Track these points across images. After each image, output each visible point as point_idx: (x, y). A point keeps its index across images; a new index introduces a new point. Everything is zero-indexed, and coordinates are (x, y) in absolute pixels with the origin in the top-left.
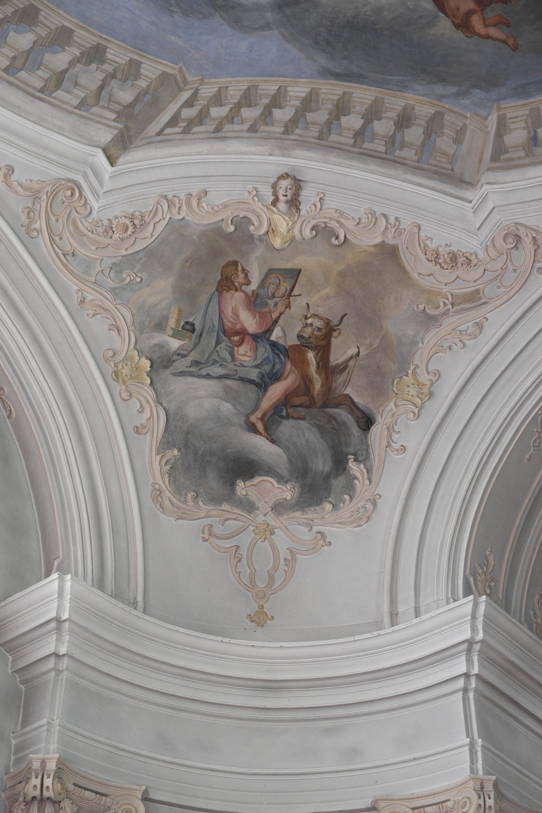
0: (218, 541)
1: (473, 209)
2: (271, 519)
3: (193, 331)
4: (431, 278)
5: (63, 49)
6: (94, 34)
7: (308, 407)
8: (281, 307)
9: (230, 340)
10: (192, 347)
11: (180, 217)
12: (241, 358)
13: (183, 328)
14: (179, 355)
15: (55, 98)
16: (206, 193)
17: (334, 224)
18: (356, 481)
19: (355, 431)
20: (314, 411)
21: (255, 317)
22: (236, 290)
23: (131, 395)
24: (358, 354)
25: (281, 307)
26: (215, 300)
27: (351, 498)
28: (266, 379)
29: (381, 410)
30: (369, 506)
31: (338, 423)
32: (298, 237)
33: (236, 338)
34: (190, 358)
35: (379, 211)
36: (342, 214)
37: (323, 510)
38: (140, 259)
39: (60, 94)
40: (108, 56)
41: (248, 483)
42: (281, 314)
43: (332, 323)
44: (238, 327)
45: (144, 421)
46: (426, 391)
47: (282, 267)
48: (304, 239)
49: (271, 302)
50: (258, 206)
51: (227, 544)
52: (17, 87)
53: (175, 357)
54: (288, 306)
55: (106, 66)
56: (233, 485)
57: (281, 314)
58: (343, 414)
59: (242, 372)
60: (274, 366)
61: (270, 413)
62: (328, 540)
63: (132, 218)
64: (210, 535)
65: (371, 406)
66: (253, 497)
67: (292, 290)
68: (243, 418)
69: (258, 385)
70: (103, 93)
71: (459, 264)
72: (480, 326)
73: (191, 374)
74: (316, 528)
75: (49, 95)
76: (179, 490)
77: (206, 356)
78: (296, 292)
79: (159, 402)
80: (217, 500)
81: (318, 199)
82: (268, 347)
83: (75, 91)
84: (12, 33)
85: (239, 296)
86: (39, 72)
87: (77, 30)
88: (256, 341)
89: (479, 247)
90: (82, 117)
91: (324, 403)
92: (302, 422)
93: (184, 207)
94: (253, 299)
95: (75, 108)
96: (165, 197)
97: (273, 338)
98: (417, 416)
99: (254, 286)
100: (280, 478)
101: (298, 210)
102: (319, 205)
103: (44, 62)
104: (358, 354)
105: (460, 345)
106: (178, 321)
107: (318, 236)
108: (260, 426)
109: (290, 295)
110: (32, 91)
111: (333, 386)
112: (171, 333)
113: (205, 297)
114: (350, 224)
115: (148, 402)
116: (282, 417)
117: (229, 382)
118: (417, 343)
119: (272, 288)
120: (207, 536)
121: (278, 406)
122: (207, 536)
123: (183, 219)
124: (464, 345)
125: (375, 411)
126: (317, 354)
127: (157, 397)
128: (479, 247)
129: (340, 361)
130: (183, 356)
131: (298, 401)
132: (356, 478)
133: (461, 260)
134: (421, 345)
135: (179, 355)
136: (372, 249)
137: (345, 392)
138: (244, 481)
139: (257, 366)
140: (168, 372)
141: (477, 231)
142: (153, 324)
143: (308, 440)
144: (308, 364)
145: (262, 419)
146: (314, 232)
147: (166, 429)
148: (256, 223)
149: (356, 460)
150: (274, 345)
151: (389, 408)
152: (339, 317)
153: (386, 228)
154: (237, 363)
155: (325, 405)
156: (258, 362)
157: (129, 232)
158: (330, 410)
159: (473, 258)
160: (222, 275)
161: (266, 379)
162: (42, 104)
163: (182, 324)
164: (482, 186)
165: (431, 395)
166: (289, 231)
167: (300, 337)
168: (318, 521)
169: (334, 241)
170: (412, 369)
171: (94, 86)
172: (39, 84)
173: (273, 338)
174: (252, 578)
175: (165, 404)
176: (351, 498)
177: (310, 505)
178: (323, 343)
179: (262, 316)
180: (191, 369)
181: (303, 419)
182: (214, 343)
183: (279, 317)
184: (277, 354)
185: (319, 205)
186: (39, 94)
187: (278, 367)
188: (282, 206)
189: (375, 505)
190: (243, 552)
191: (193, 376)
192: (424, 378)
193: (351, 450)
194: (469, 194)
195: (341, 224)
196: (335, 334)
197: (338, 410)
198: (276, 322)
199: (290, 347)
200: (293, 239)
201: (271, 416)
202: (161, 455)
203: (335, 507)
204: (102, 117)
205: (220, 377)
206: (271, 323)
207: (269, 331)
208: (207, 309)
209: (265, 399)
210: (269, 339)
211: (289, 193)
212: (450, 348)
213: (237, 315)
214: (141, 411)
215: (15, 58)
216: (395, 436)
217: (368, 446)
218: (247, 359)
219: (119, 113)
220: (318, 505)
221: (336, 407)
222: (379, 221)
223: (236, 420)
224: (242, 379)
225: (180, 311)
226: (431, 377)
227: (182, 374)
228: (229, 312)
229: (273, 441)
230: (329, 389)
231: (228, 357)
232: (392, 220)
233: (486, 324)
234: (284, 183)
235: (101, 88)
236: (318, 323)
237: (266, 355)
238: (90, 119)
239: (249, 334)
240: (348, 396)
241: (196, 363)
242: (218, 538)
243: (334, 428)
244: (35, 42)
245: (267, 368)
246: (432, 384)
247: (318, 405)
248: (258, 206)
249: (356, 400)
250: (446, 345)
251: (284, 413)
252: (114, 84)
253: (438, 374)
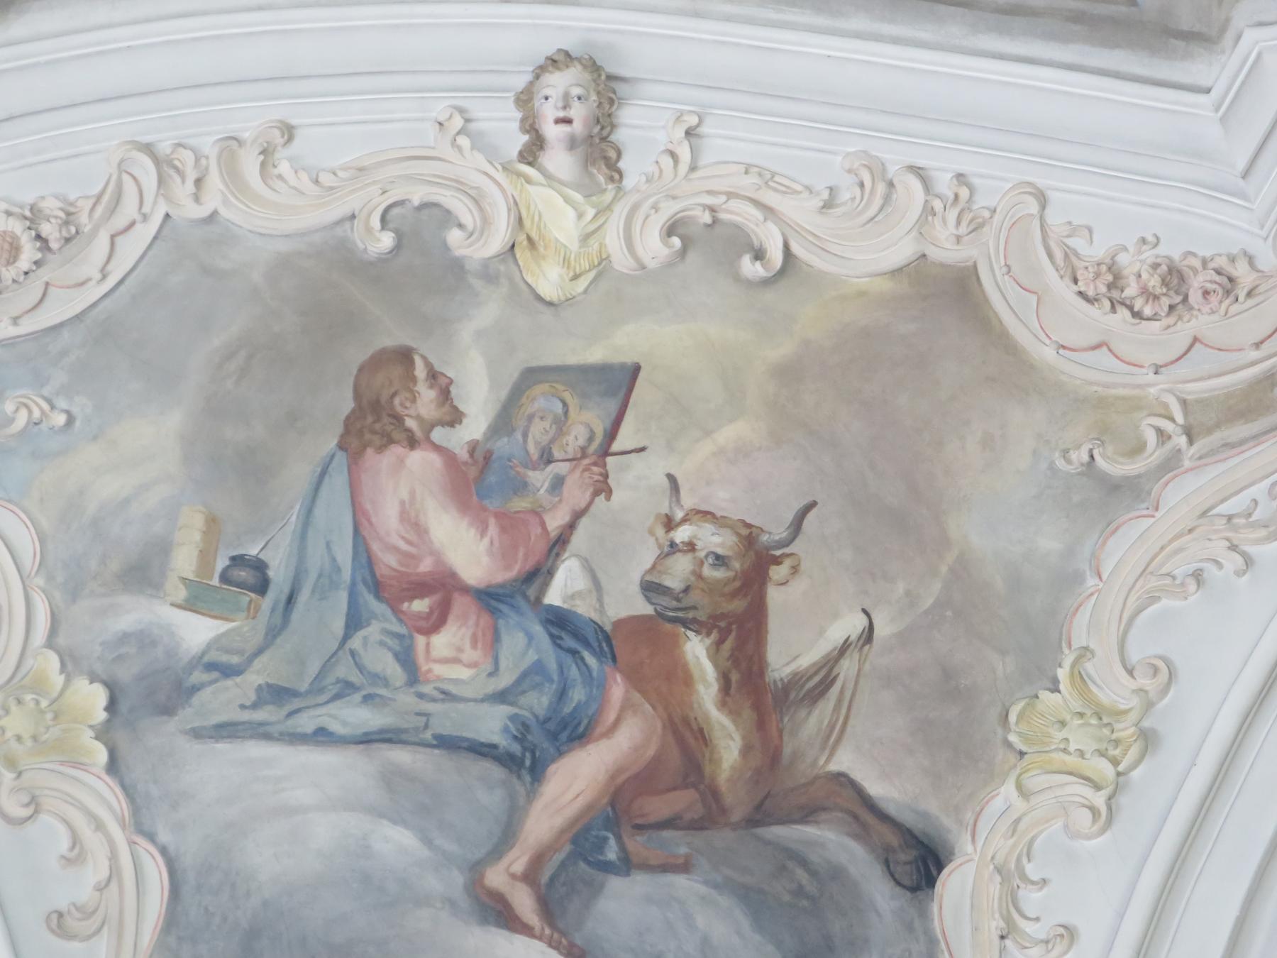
1: (1217, 110)
3: (262, 587)
4: (1103, 357)
7: (697, 826)
8: (575, 493)
9: (396, 611)
10: (258, 638)
11: (202, 212)
12: (439, 670)
13: (225, 578)
14: (211, 667)
16: (289, 132)
17: (741, 213)
20: (721, 838)
21: (483, 532)
22: (412, 443)
23: (35, 804)
24: (868, 634)
25: (575, 493)
26: (338, 481)
28: (536, 737)
29: (969, 816)
31: (813, 873)
32: (621, 261)
33: (420, 606)
34: (254, 678)
35: (895, 158)
36: (768, 178)
38: (64, 353)
42: (578, 515)
43: (764, 538)
44: (426, 566)
45: (85, 894)
46: (1125, 730)
47: (572, 360)
48: (643, 267)
49: (540, 479)
50: (471, 167)
53: (198, 676)
54: (603, 488)
57: (578, 515)
59: (447, 720)
60: (562, 694)
61: (559, 857)
63: (33, 217)
65: (932, 806)
67: (612, 434)
68: (459, 878)
69: (509, 761)
71: (1195, 297)
73: (261, 733)
77: (313, 668)
78: (624, 440)
79: (141, 827)
81: (680, 133)
82: (538, 629)
85: (420, 461)
88: (494, 612)
89: (1257, 230)
91: (759, 807)
92: (681, 883)
93: (214, 181)
94: (473, 472)
96: (148, 149)
97: (554, 597)
98: (1106, 818)
99: (475, 427)
101: (615, 174)
102: (685, 153)
104: (868, 634)
106: (206, 558)
107: (692, 256)
108: (524, 902)
109: (605, 452)
111: (787, 751)
112: (181, 594)
113: (299, 473)
114: (799, 210)
115: (99, 826)
116: (607, 867)
117: (401, 756)
118: (1078, 578)
119: (539, 432)
121: (587, 829)
123: (213, 217)
124: (1248, 561)
125: (947, 821)
126: (719, 643)
127: (136, 810)
128: (1257, 230)
129: (806, 661)
130: (228, 671)
131: (658, 807)
133: (1196, 284)
134: (1091, 582)
135: (211, 667)
136: (886, 285)
137: (834, 767)
139: (501, 697)
140: (172, 725)
141: (1241, 183)
142: (114, 566)
143: (705, 942)
144: (687, 680)
145: (529, 877)
146: (676, 242)
147: (171, 921)
148: (467, 219)
150: (559, 622)
151: (997, 804)
152: (789, 516)
153: (929, 211)
154: (427, 689)
155: (759, 816)
156: (505, 679)
157: (24, 263)
159: (1241, 270)
160: (357, 395)
161: (536, 737)
163: (221, 563)
164: (1239, 37)
165: (1148, 740)
166: (585, 238)
167: (650, 588)
169: (751, 269)
170: (1067, 663)
173: (554, 597)
175: (164, 837)
178: (738, 605)
179: (509, 523)
180: (260, 715)
181: (684, 867)
182: (338, 625)
183: (571, 526)
184: (574, 652)
185: (685, 153)
187: (578, 694)
188: (559, 160)
191: (267, 737)
194: (1196, 69)
195: (768, 211)
196: (777, 572)
197: (810, 831)
198: (560, 542)
199: (618, 624)
200: (603, 266)
201: (563, 865)
205: (367, 740)
206: (540, 547)
207: (539, 574)
208: (309, 512)
209: (538, 805)
210: (538, 600)
211: (578, 112)
212: (1198, 576)
213: (418, 528)
214: (76, 856)
216: (1031, 899)
218: (464, 673)
221: (803, 820)
222: (899, 193)
223: (432, 883)
224: (447, 744)
225: (212, 524)
226: (1144, 681)
227: (227, 731)
228: (387, 518)
230: (774, 758)
231: (394, 671)
232: (944, 183)
234: (558, 83)
236: (712, 539)
237: (532, 656)
239: (466, 589)
240: (842, 779)
241: (276, 694)
243: (799, 892)
245: (538, 702)
246: (1149, 706)
247: (737, 816)
248: (471, 167)
249: (875, 789)
250: (1181, 568)
251: (612, 854)
253: (1166, 671)
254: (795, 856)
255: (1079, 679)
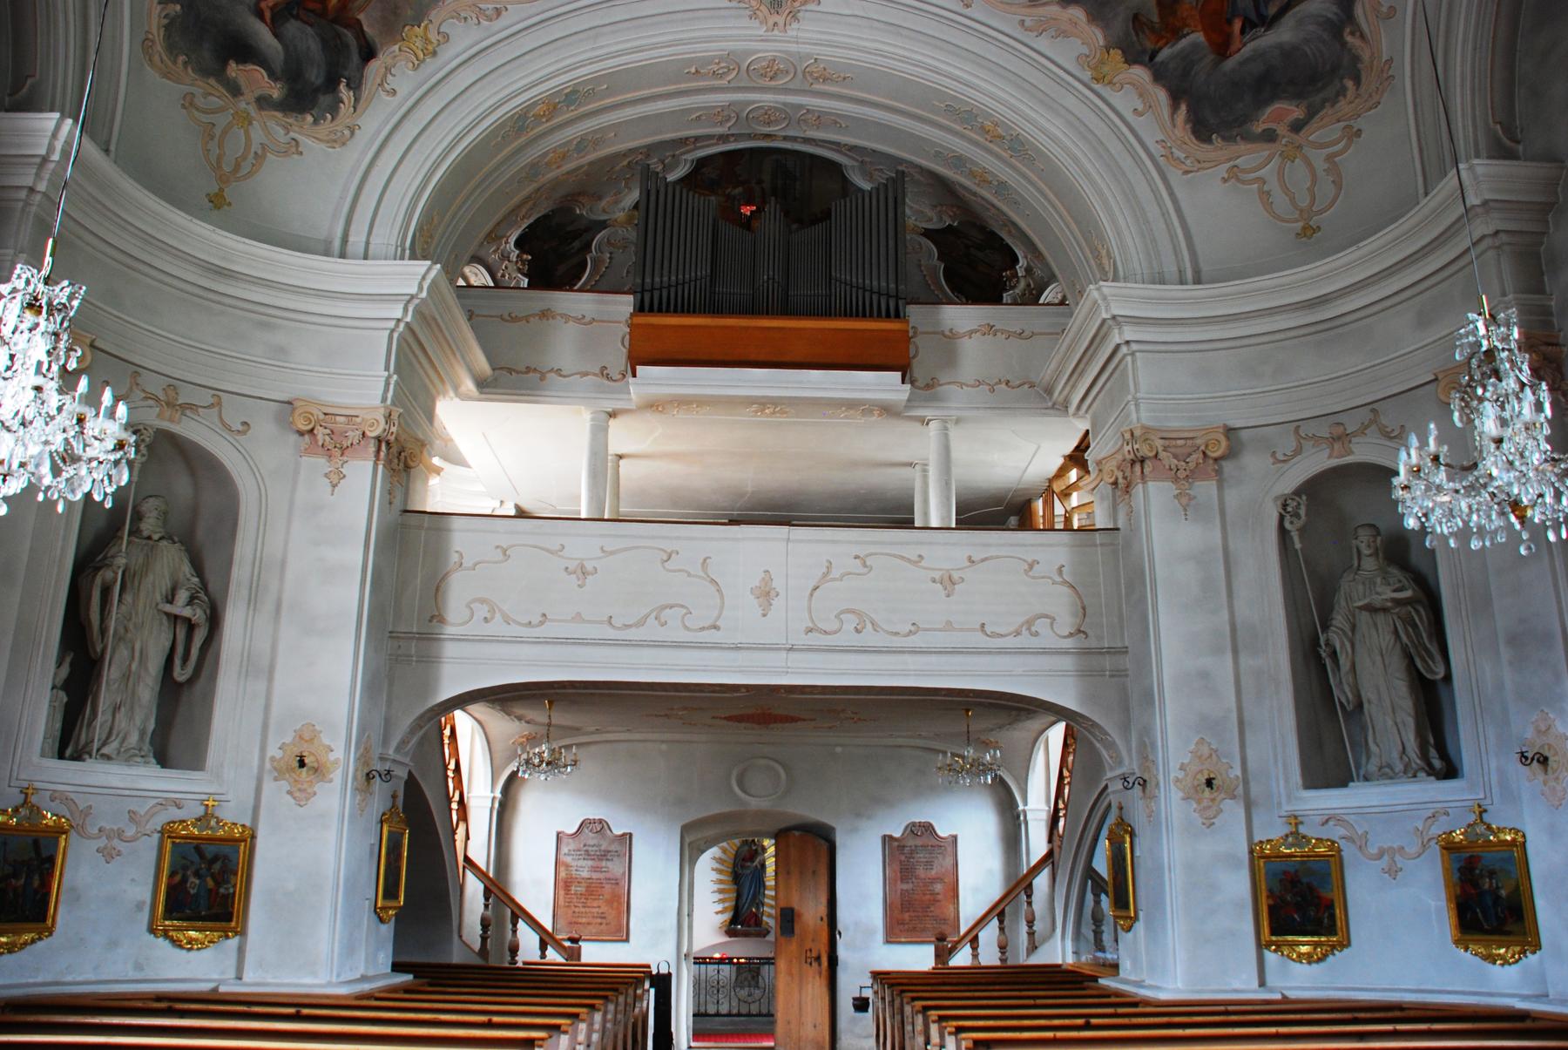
0: (196, 113)
2: (252, 110)
18: (342, 105)
19: (355, 58)
27: (333, 119)
30: (347, 132)
37: (304, 119)
41: (241, 67)
51: (205, 118)
56: (225, 63)
58: (349, 36)
62: (300, 149)
64: (191, 104)
65: (377, 40)
66: (242, 82)
72: (498, 12)
74: (292, 134)
76: (171, 48)
80: (205, 72)
92: (309, 28)
98: (415, 68)
100: (272, 75)
105: (475, 21)
108: (268, 15)
116: (293, 17)
120: (187, 105)
122: (187, 105)
124: (479, 23)
125: (379, 46)
132: (342, 102)
137: (359, 17)
138: (237, 63)
143: (308, 48)
145: (272, 9)
149: (348, 85)
155: (335, 21)
158: (338, 27)
165: (434, 53)
168: (296, 129)
170: (426, 22)
174: (219, 158)
176: (333, 119)
177: (293, 110)
181: (311, 25)
189: (352, 133)
190: (218, 131)
192: (433, 36)
193: (346, 73)
197: (345, 31)
202: (162, 6)
203: (316, 122)
212: (465, 18)
216: (390, 78)
217: (362, 76)
220: (300, 113)
221: (345, 28)
226: (440, 39)
229: (276, 35)
233: (504, 13)
240: (359, 22)
242: (197, 109)
246: (439, 45)
249: (365, 28)
250: (463, 14)
251: (295, 12)
253: (447, 37)
254: (339, 36)
255: (426, 27)
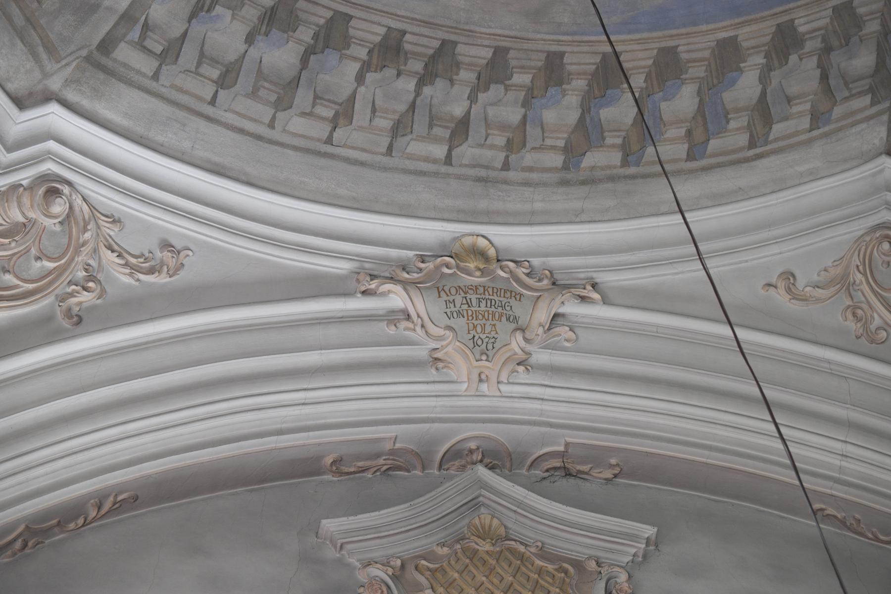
5: (741, 71)
6: (763, 19)
15: (777, 140)
39: (778, 129)
40: (802, 29)
52: (719, 165)
55: (810, 45)
70: (832, 82)
75: (766, 143)
83: (795, 109)
84: (664, 105)
86: (732, 125)
87: (740, 32)
90: (826, 135)
95: (811, 130)
103: (729, 106)
110: (740, 155)
162: (765, 162)
171: (814, 84)
172: (743, 139)
186: (751, 153)
204: (853, 113)
215: (689, 133)
219: (871, 90)
235: (824, 77)
238: (840, 129)
244: (699, 92)
252: (836, 58)
